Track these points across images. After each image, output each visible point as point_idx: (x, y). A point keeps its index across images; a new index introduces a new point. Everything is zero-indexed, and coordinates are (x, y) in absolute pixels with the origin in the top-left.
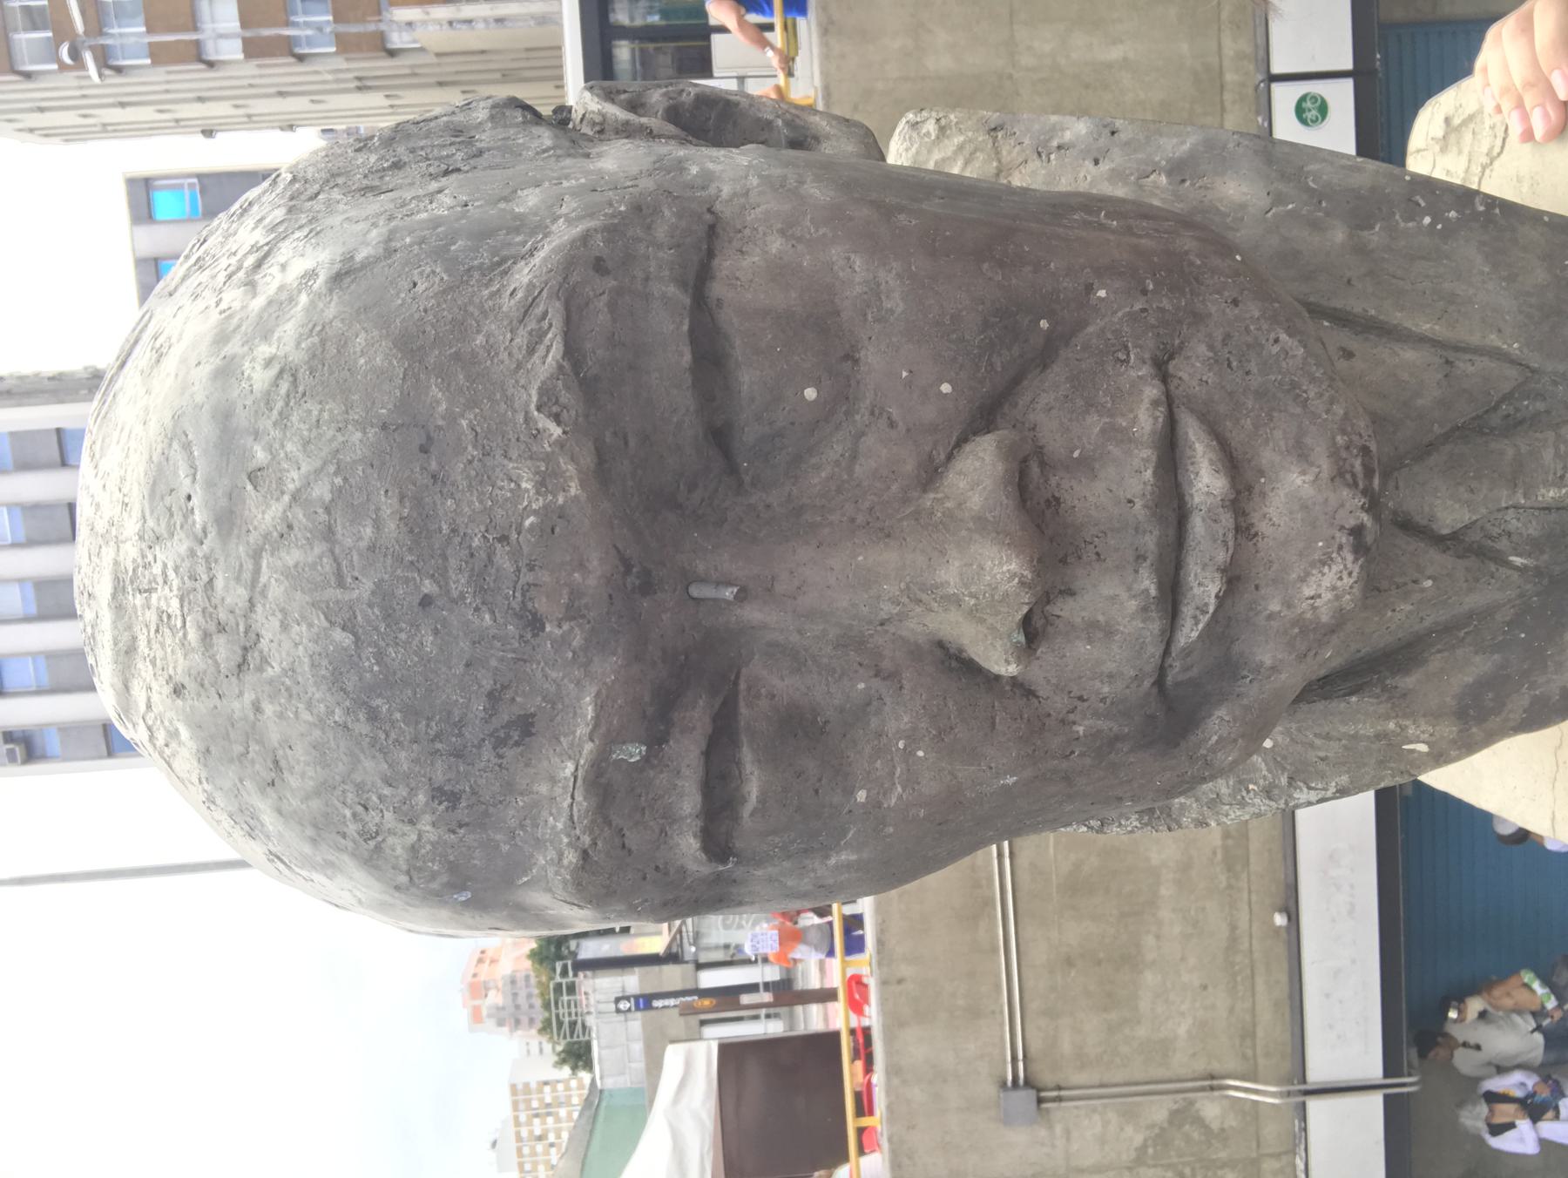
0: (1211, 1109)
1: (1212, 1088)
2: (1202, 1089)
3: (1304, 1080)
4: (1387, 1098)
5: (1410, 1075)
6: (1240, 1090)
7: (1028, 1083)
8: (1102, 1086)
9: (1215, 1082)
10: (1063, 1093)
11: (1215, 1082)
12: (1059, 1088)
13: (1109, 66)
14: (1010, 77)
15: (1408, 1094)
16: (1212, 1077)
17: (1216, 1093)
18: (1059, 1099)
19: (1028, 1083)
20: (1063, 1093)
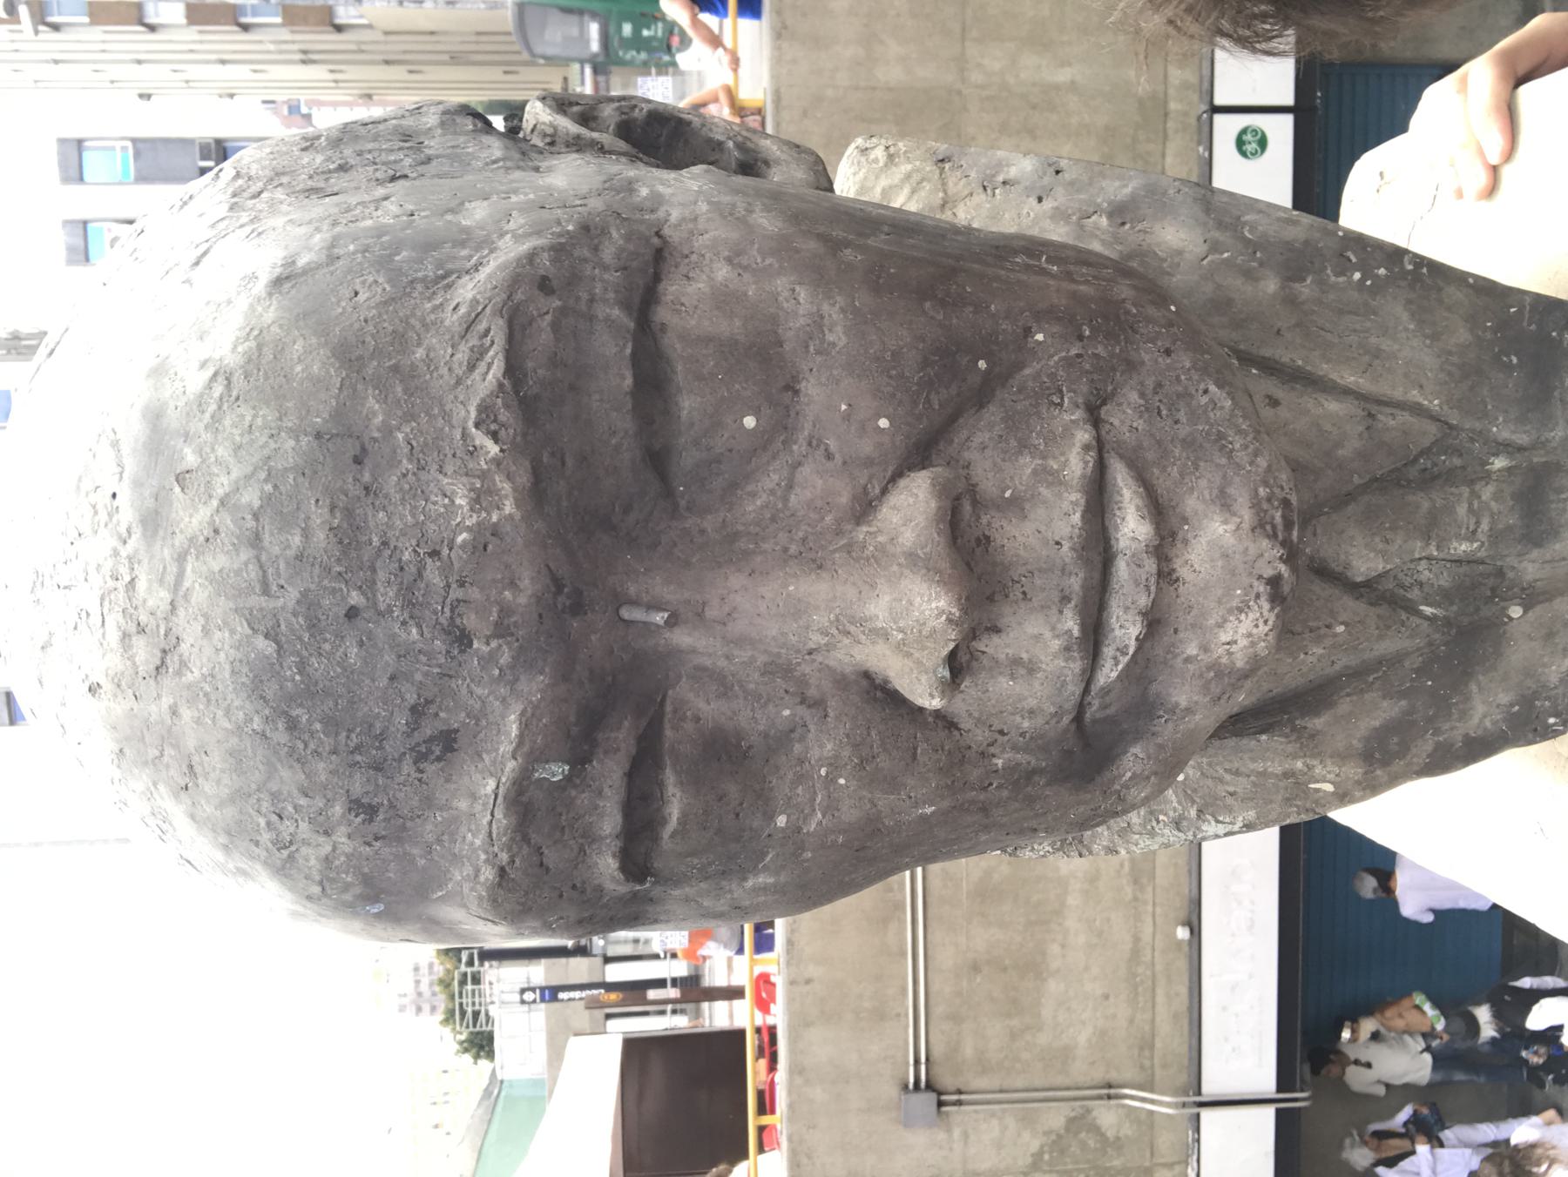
0: (1107, 1117)
1: (1109, 1097)
2: (1100, 1097)
3: (1199, 1093)
4: (1279, 1112)
5: (1302, 1090)
6: (1136, 1100)
7: (930, 1086)
8: (1001, 1091)
9: (1112, 1091)
10: (963, 1097)
11: (1112, 1091)
12: (960, 1092)
15: (1299, 1109)
17: (1113, 1102)
18: (959, 1103)
19: (930, 1086)
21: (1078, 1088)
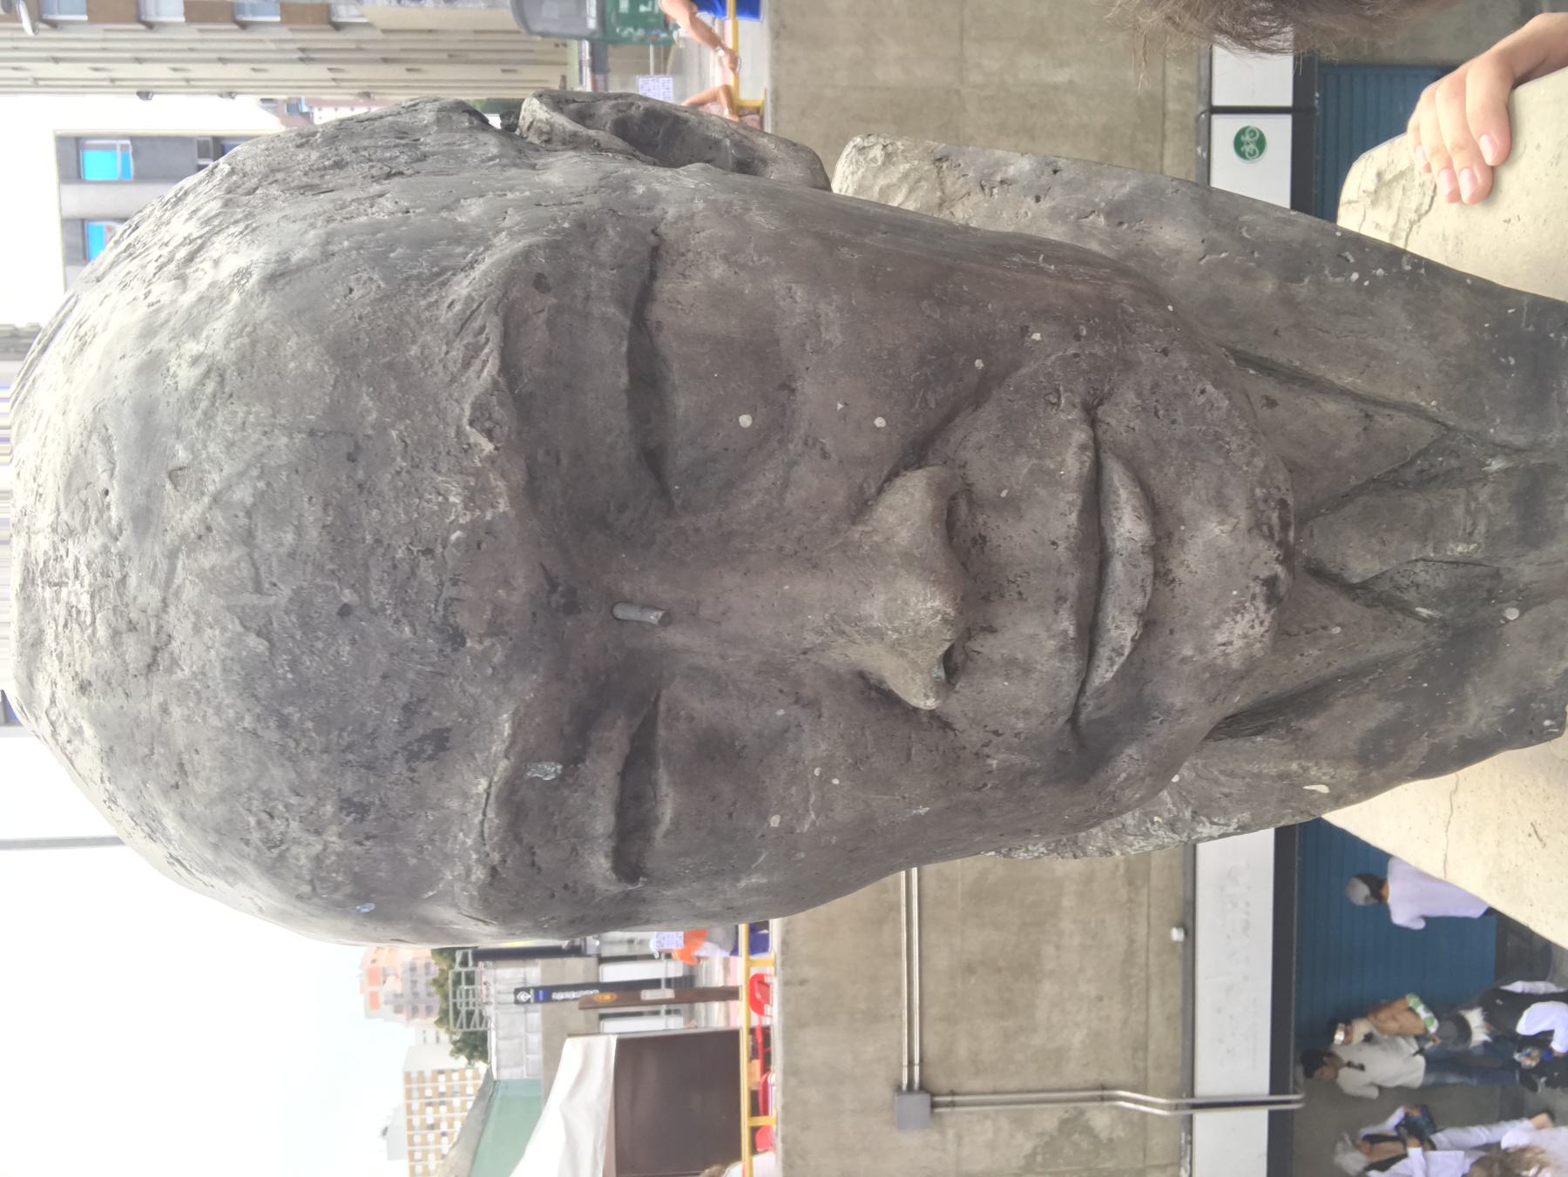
0: (1100, 1119)
1: (1103, 1099)
2: (1093, 1099)
3: (1192, 1095)
4: (1272, 1114)
6: (1130, 1101)
8: (995, 1093)
9: (1106, 1093)
10: (957, 1098)
11: (1106, 1093)
13: (1056, 88)
14: (958, 92)
15: (1292, 1111)
16: (1103, 1088)
17: (1106, 1104)
18: (952, 1104)
20: (957, 1098)
21: (1071, 1090)
